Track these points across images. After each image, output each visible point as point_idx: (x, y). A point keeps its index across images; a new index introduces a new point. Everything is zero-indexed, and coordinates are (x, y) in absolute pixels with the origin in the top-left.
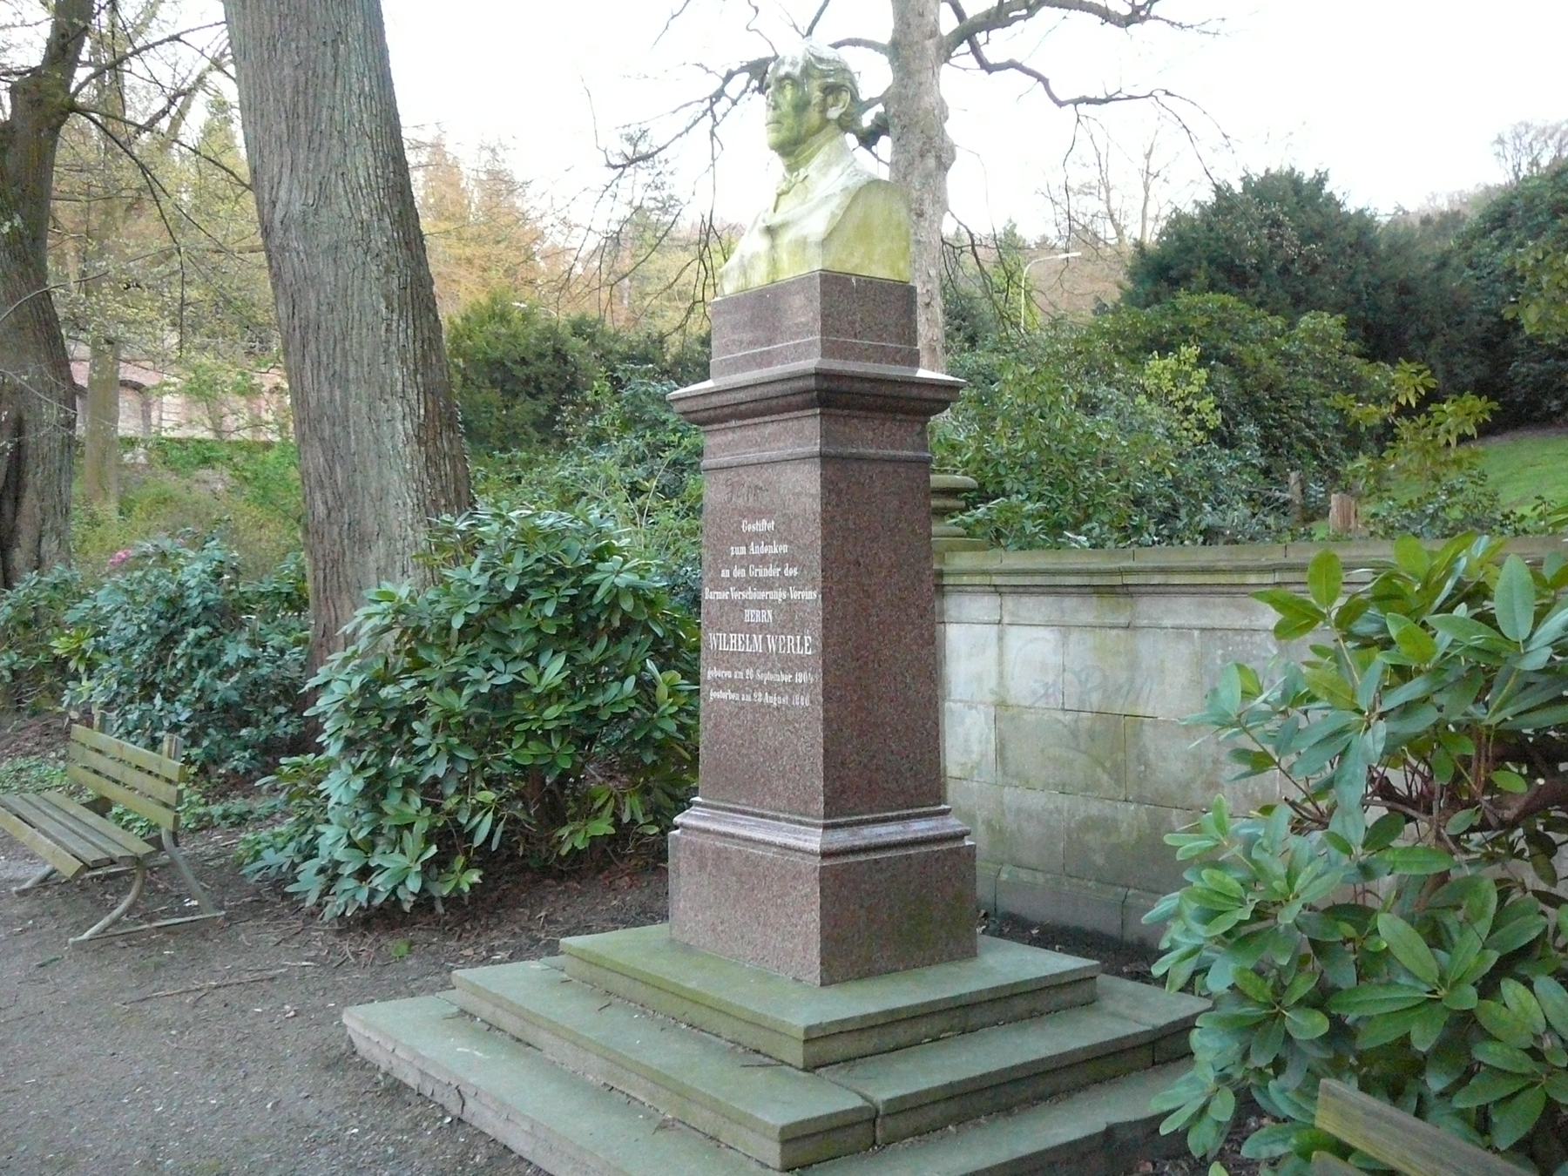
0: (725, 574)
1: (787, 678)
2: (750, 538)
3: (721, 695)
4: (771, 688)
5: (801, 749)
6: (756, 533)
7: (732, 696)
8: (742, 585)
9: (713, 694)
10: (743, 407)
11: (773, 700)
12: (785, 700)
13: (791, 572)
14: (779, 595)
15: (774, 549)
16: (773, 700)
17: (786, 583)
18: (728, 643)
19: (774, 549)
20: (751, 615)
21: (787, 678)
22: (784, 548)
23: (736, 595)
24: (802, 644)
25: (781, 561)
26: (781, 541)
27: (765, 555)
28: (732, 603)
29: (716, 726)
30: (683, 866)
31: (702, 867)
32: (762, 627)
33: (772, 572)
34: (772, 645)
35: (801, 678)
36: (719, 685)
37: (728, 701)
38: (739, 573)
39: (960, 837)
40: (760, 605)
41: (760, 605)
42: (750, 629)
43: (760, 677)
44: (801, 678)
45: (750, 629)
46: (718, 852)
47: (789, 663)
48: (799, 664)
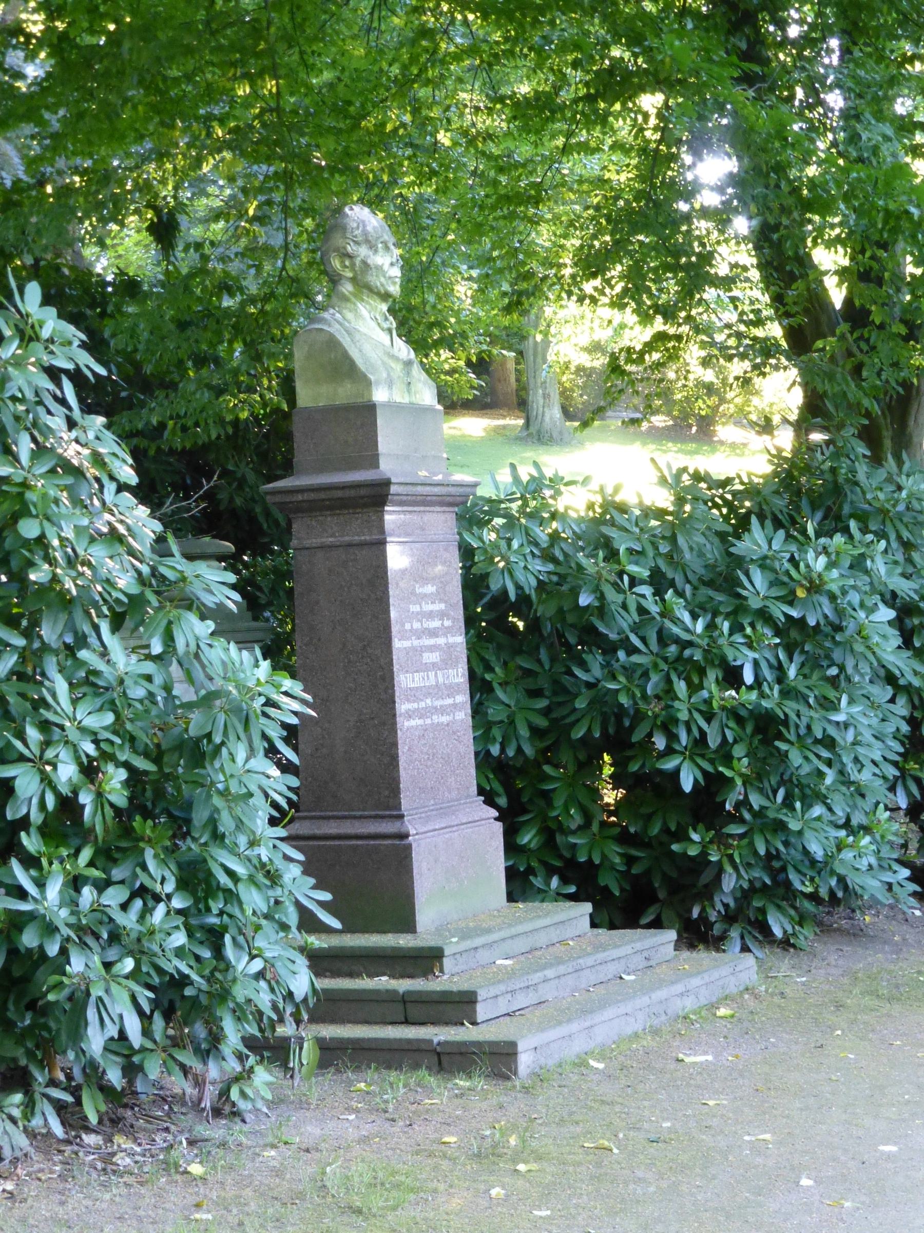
0: (408, 626)
1: (450, 701)
3: (413, 723)
4: (442, 710)
6: (426, 595)
7: (420, 722)
11: (444, 719)
14: (441, 641)
16: (444, 719)
21: (450, 701)
23: (416, 643)
26: (441, 601)
28: (414, 649)
33: (436, 624)
34: (441, 680)
36: (409, 715)
38: (417, 625)
40: (432, 649)
41: (432, 649)
45: (426, 668)
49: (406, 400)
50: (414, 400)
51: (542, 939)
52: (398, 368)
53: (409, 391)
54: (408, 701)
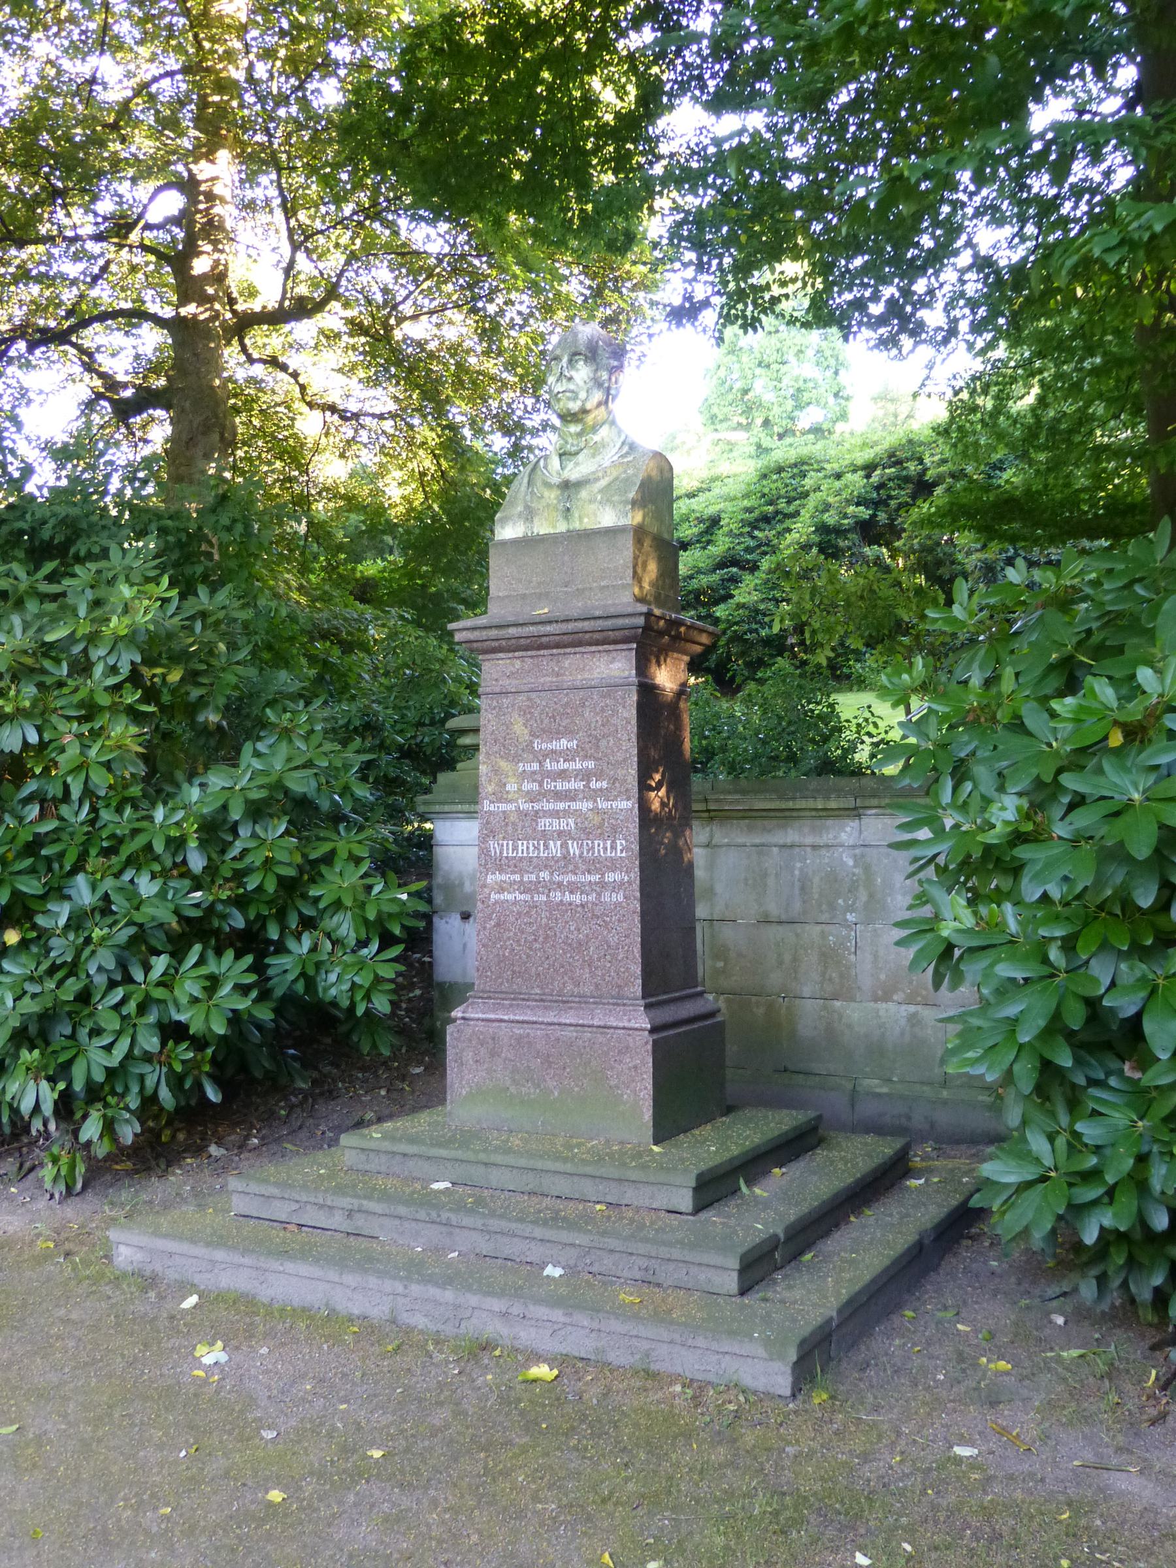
2: (545, 756)
4: (573, 888)
5: (613, 939)
11: (577, 898)
12: (592, 897)
13: (594, 785)
15: (577, 765)
16: (577, 898)
17: (593, 795)
18: (515, 848)
19: (577, 765)
20: (544, 823)
22: (591, 764)
23: (525, 806)
24: (613, 848)
25: (586, 776)
26: (586, 757)
29: (498, 925)
30: (469, 1056)
31: (493, 1054)
33: (574, 785)
35: (610, 877)
37: (515, 903)
39: (712, 1014)
40: (556, 814)
41: (556, 814)
42: (545, 836)
43: (557, 878)
44: (610, 877)
46: (519, 1039)
47: (594, 865)
48: (613, 865)
49: (562, 527)
50: (576, 525)
51: (561, 1186)
52: (552, 496)
53: (566, 518)
54: (501, 871)
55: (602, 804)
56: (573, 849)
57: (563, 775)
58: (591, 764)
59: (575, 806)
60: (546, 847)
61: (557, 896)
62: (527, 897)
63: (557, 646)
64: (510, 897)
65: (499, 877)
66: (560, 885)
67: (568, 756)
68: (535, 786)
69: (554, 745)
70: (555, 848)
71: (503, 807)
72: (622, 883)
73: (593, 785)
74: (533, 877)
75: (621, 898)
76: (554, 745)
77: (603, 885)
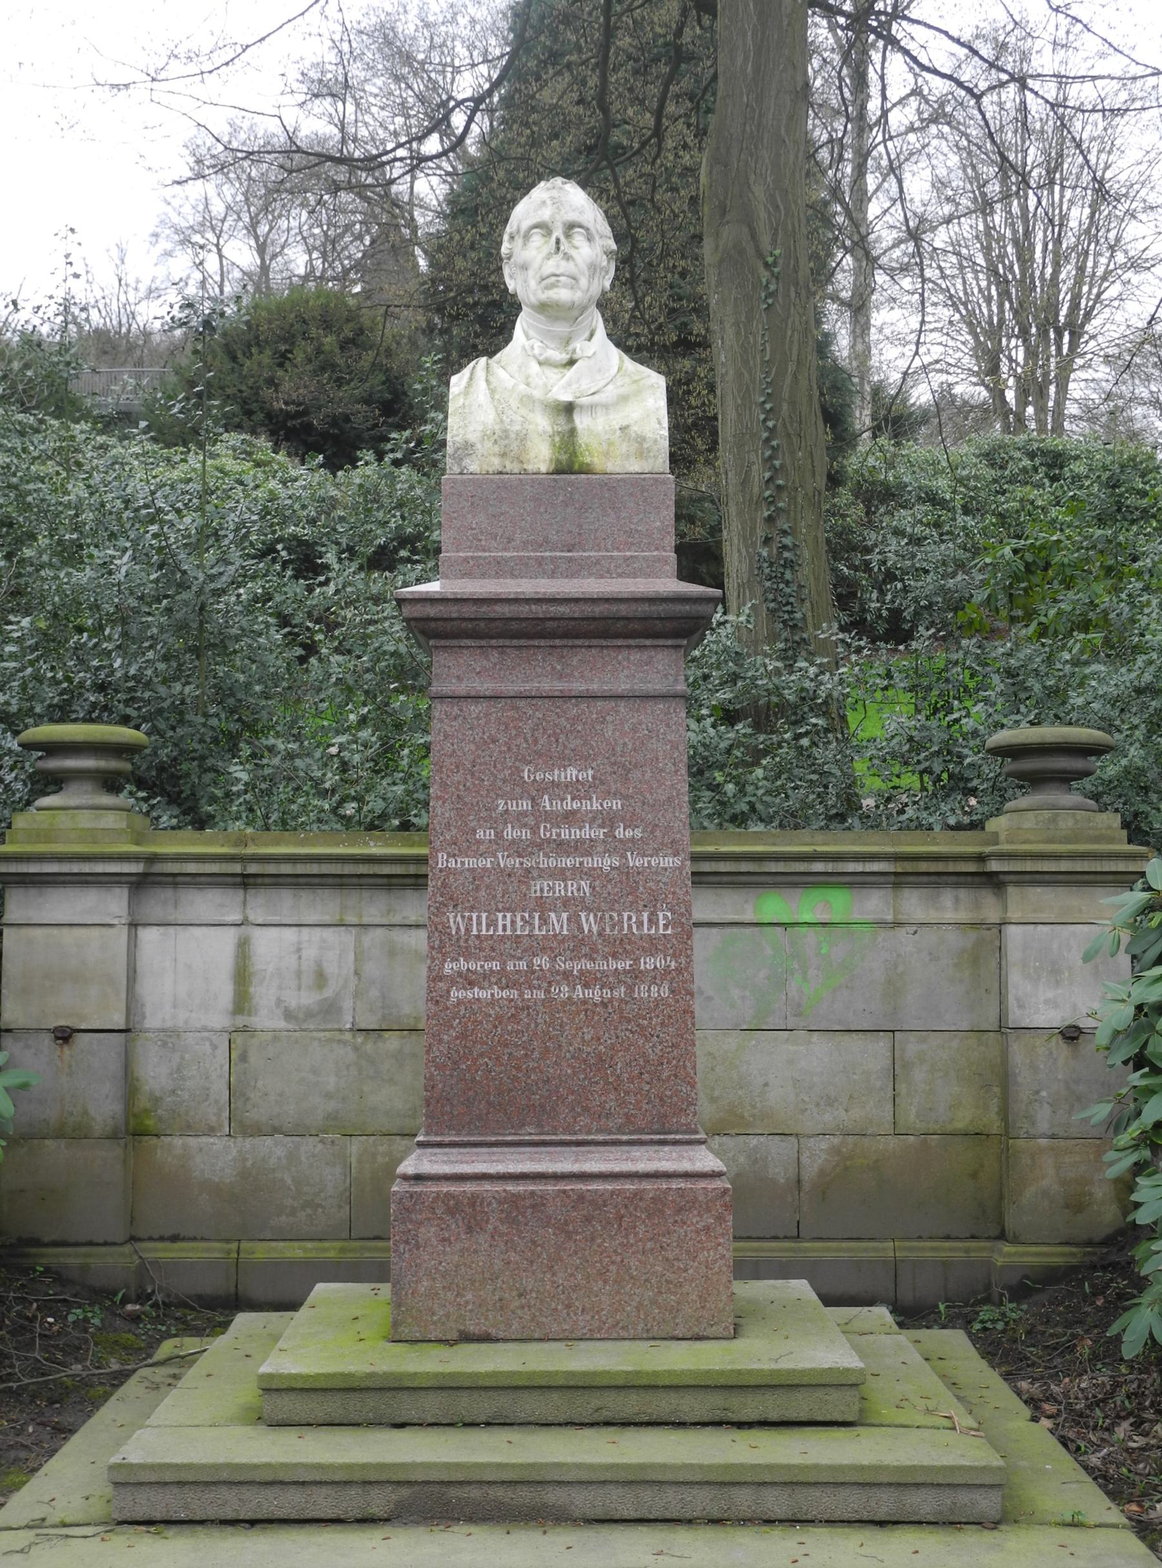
8: (518, 849)
9: (456, 994)
10: (549, 624)
11: (595, 994)
14: (607, 863)
16: (595, 994)
17: (620, 848)
18: (492, 923)
20: (539, 887)
22: (616, 804)
24: (653, 921)
26: (608, 794)
27: (573, 813)
29: (463, 1036)
32: (566, 902)
33: (587, 833)
35: (648, 963)
37: (493, 1002)
40: (561, 874)
42: (543, 906)
43: (562, 966)
44: (648, 963)
47: (620, 946)
54: (468, 957)
55: (635, 861)
56: (589, 923)
57: (569, 818)
58: (616, 804)
59: (589, 863)
60: (544, 921)
61: (563, 991)
62: (514, 994)
63: (565, 635)
64: (483, 994)
65: (463, 965)
66: (567, 975)
67: (578, 790)
68: (526, 834)
69: (556, 775)
70: (559, 923)
71: (470, 862)
72: (667, 971)
73: (620, 833)
74: (523, 965)
75: (665, 992)
76: (556, 775)
77: (636, 974)
